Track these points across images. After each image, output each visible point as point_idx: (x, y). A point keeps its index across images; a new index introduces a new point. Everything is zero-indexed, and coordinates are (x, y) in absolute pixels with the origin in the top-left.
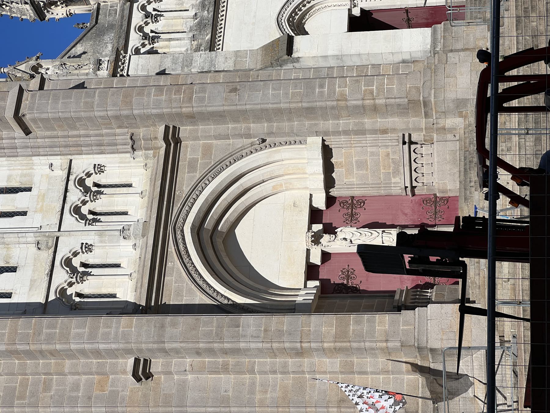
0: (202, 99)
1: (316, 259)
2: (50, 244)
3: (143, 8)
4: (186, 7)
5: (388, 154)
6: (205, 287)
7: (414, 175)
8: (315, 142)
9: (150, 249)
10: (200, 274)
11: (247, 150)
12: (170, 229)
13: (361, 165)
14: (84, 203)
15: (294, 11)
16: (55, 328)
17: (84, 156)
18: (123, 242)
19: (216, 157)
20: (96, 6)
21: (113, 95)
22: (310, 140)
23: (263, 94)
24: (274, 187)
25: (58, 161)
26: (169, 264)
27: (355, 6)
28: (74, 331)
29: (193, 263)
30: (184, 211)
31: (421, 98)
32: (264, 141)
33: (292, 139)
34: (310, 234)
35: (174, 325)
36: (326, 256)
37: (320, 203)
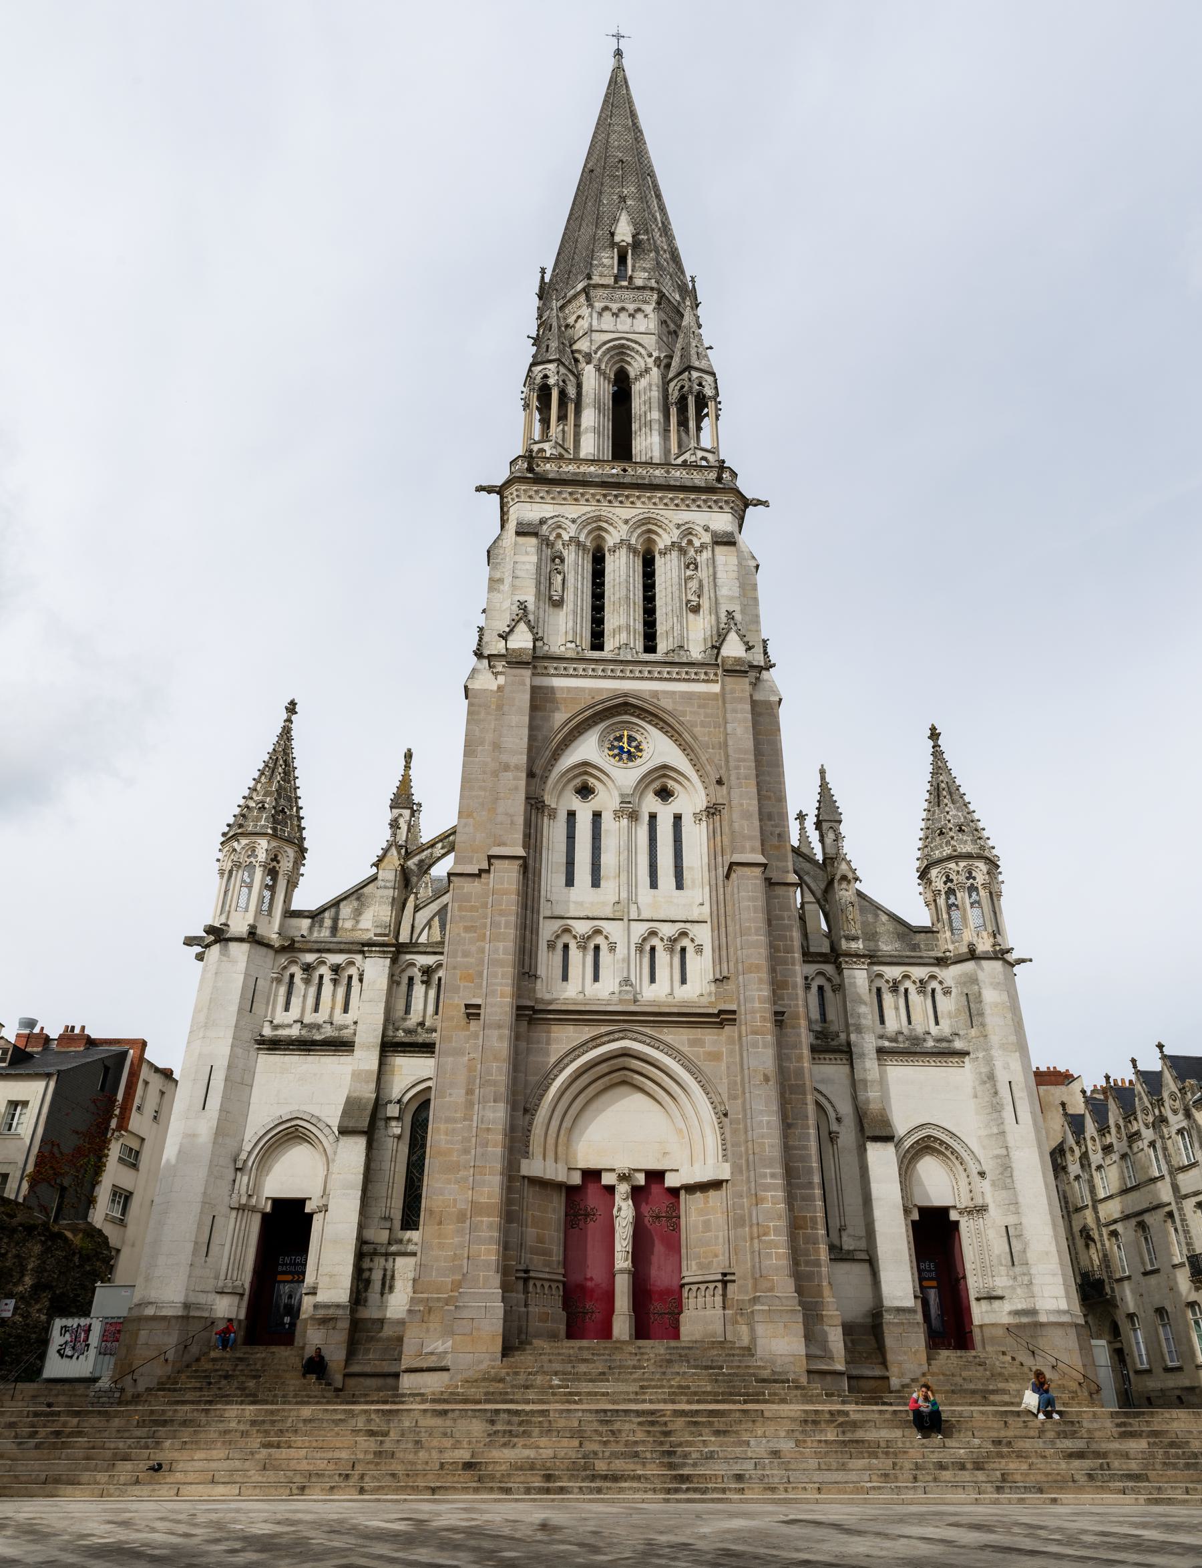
0: (755, 1045)
1: (608, 1179)
2: (617, 914)
3: (933, 977)
4: (941, 1021)
5: (716, 1256)
6: (560, 1064)
7: (694, 1287)
8: (724, 1172)
9: (588, 1008)
10: (575, 1060)
11: (714, 1099)
12: (626, 1026)
13: (707, 1225)
14: (662, 939)
15: (942, 1143)
16: (506, 928)
17: (710, 934)
18: (617, 981)
19: (707, 1067)
20: (935, 929)
21: (759, 953)
22: (727, 1166)
23: (762, 1111)
24: (681, 1130)
25: (705, 912)
26: (587, 1028)
27: (960, 1213)
28: (501, 945)
29: (587, 1051)
30: (644, 1038)
31: (758, 1294)
32: (726, 1115)
33: (729, 1146)
34: (626, 1172)
35: (500, 1038)
36: (611, 1189)
37: (671, 1181)
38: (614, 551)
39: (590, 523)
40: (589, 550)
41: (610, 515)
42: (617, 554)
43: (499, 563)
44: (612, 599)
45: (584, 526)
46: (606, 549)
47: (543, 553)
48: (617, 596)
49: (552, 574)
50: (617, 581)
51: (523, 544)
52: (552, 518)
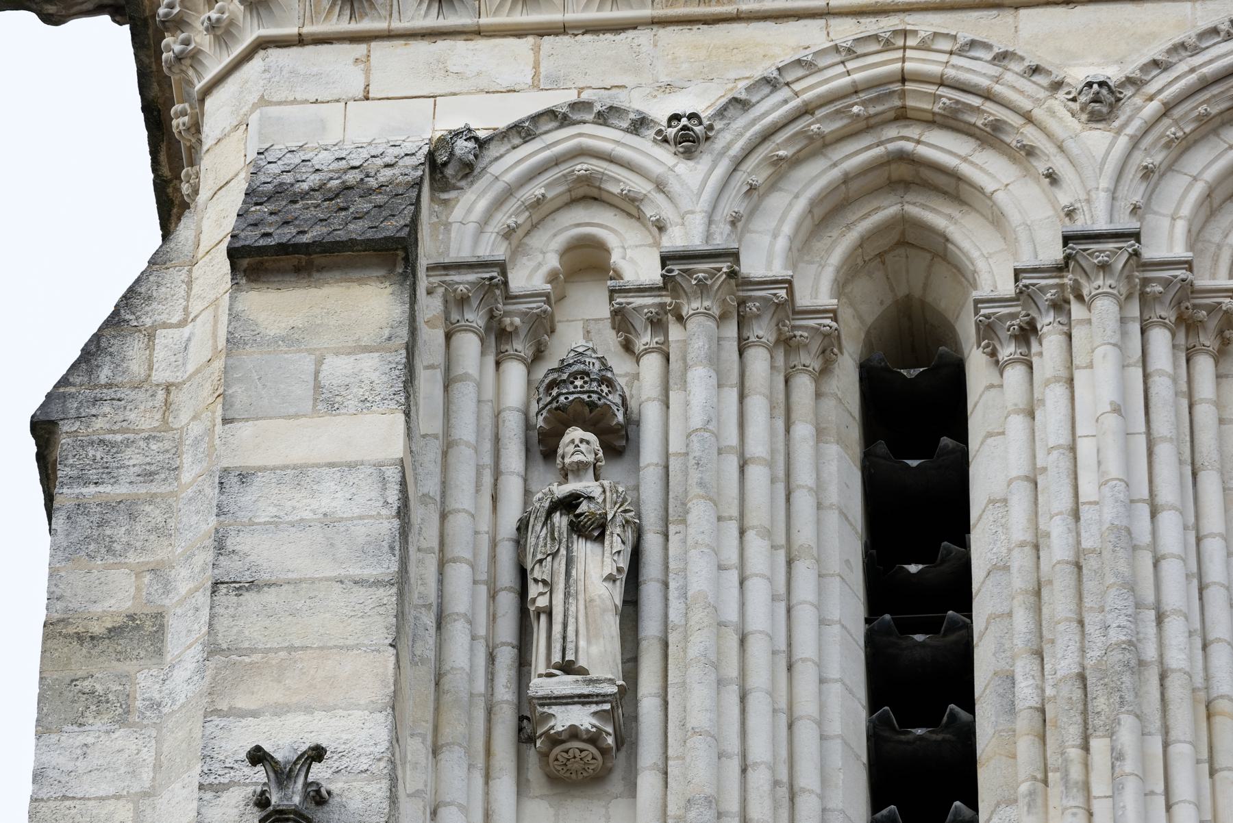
38: (1027, 333)
39: (818, 146)
40: (829, 346)
41: (977, 71)
42: (1049, 347)
43: (130, 509)
44: (1026, 692)
45: (782, 168)
46: (967, 329)
47: (466, 396)
48: (1063, 662)
49: (538, 533)
50: (1059, 548)
51: (291, 340)
52: (522, 131)
